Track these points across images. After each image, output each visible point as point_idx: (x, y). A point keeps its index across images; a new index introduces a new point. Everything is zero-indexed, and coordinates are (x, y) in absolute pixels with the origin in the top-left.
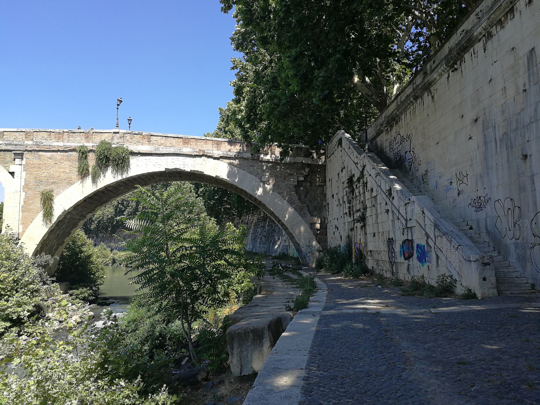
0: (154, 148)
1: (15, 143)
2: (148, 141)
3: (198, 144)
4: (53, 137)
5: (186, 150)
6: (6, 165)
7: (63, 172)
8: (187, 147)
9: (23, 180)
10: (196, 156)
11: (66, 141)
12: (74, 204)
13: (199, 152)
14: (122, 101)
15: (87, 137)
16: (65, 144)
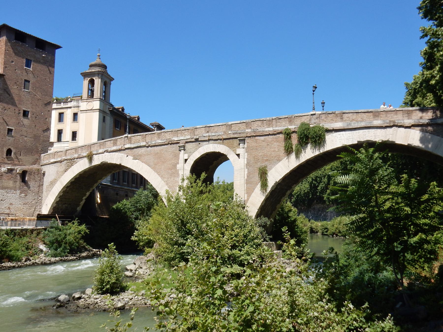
0: (346, 124)
1: (239, 132)
2: (341, 119)
3: (389, 115)
4: (265, 124)
5: (377, 122)
6: (234, 149)
7: (274, 151)
9: (246, 160)
10: (386, 127)
11: (274, 126)
12: (283, 176)
13: (390, 123)
14: (316, 88)
15: (290, 121)
16: (274, 129)
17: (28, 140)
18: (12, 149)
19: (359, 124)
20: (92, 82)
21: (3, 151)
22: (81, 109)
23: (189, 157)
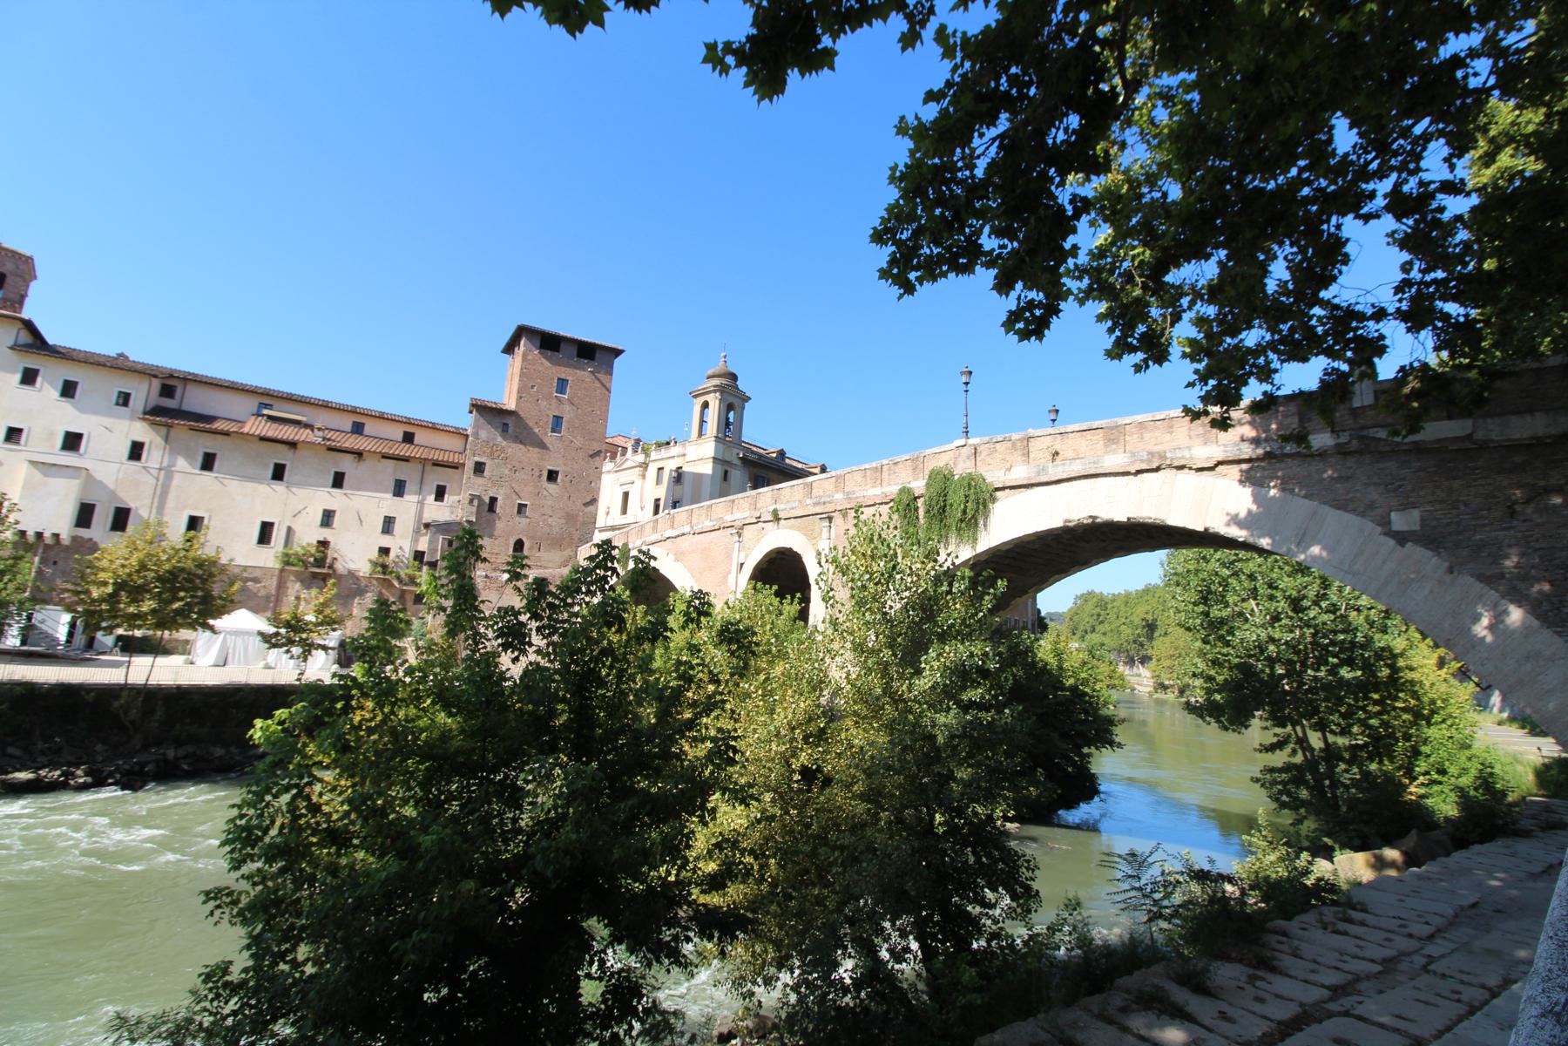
3: (1147, 436)
8: (1114, 452)
13: (1150, 461)
14: (970, 373)
15: (914, 469)
17: (556, 523)
18: (524, 540)
19: (1067, 468)
20: (706, 405)
21: (508, 545)
22: (688, 458)
23: (746, 557)
